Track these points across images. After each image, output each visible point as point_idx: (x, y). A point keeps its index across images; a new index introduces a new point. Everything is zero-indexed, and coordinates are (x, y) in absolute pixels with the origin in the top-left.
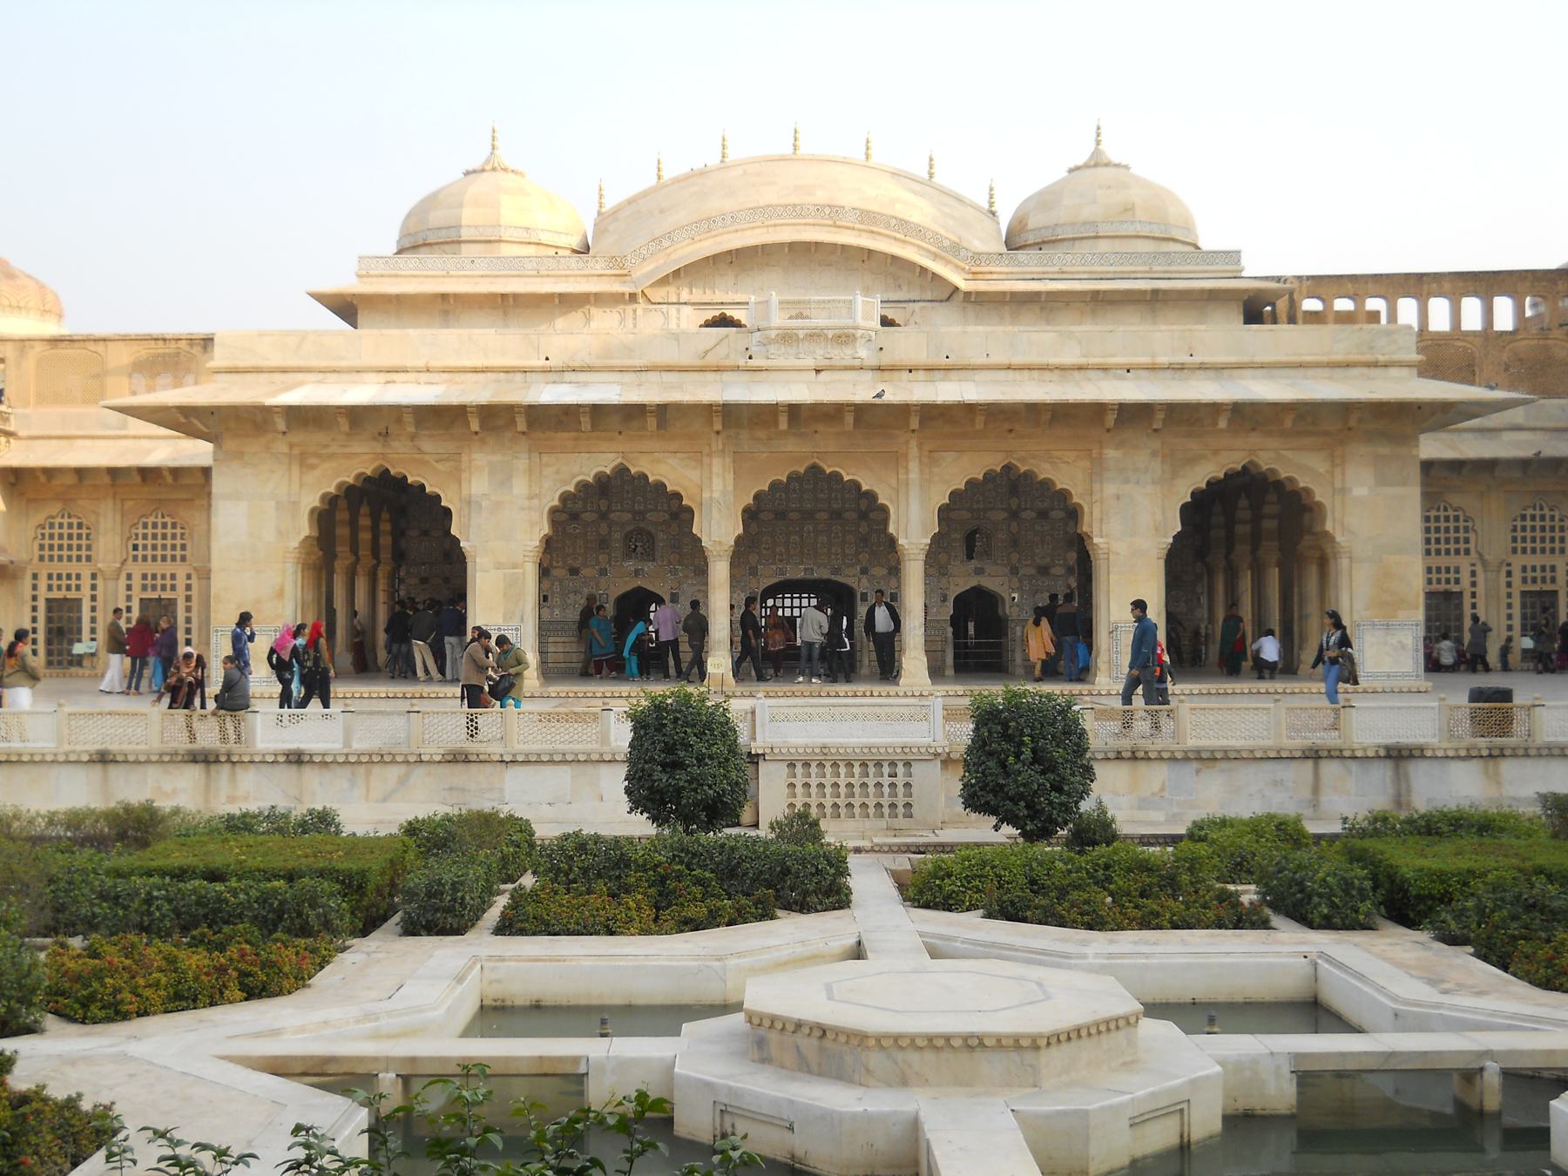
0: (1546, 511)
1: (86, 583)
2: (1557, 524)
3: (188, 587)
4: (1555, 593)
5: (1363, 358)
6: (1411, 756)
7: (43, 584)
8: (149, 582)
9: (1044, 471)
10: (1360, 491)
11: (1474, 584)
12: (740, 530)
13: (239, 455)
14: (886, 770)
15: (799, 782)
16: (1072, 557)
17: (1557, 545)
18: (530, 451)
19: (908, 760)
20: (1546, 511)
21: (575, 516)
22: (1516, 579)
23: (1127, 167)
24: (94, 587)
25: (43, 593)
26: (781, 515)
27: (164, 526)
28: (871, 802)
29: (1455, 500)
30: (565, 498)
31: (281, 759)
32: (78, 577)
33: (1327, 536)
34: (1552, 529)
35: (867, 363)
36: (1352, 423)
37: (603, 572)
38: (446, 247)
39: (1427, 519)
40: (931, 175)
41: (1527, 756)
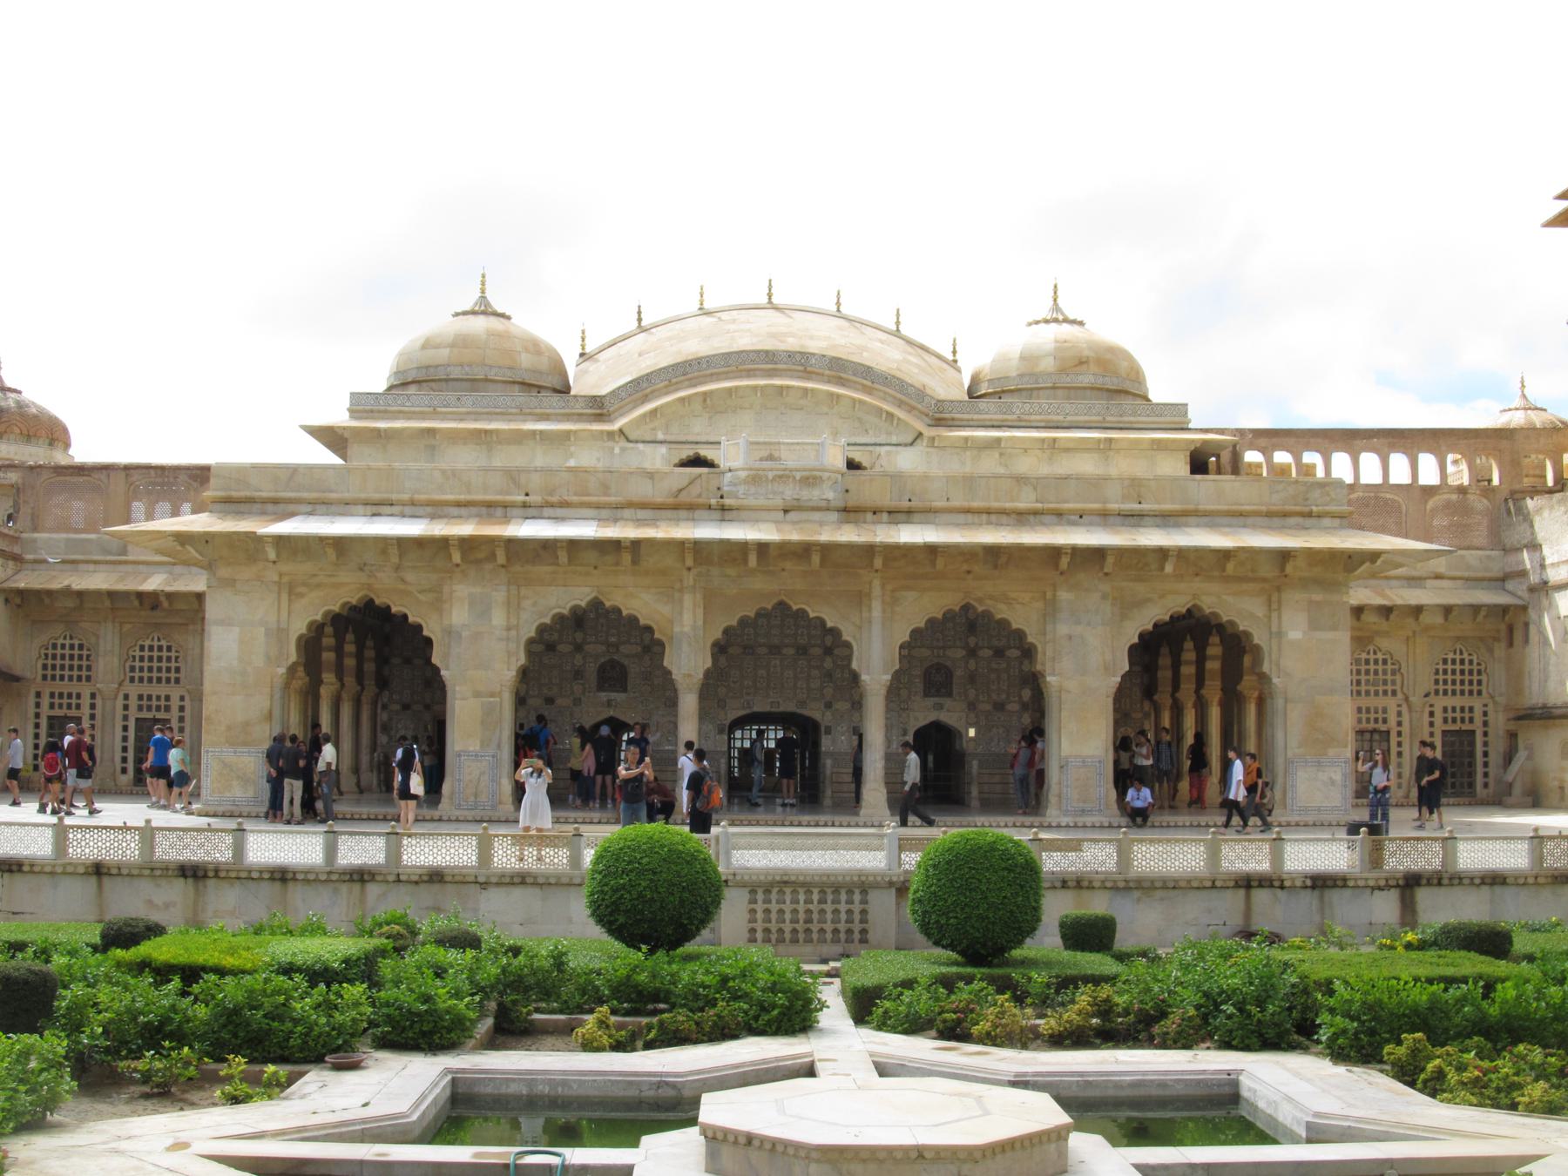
0: (1465, 656)
1: (86, 701)
2: (1475, 668)
3: (182, 709)
4: (1473, 732)
5: (1298, 508)
6: (1335, 886)
7: (45, 701)
8: (145, 702)
9: (1001, 612)
10: (1294, 635)
11: (1399, 724)
12: (709, 664)
13: (230, 583)
14: (843, 897)
15: (760, 907)
16: (1027, 694)
18: (509, 583)
19: (861, 885)
21: (551, 647)
22: (1438, 720)
23: (1081, 323)
24: (93, 706)
25: (45, 711)
26: (748, 649)
27: (160, 648)
28: (829, 927)
29: (1384, 643)
30: (542, 629)
31: (266, 876)
32: (79, 696)
33: (1263, 678)
35: (833, 504)
36: (1289, 569)
37: (577, 702)
38: (433, 384)
39: (1358, 661)
41: (1440, 884)
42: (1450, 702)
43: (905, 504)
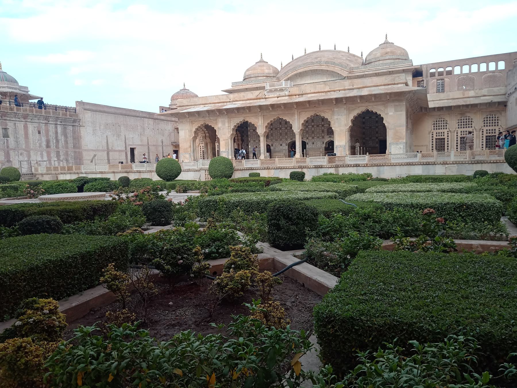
9: (322, 115)
10: (391, 114)
17: (496, 124)
20: (494, 116)
29: (468, 115)
34: (495, 120)
40: (349, 51)
42: (488, 128)
43: (301, 93)
